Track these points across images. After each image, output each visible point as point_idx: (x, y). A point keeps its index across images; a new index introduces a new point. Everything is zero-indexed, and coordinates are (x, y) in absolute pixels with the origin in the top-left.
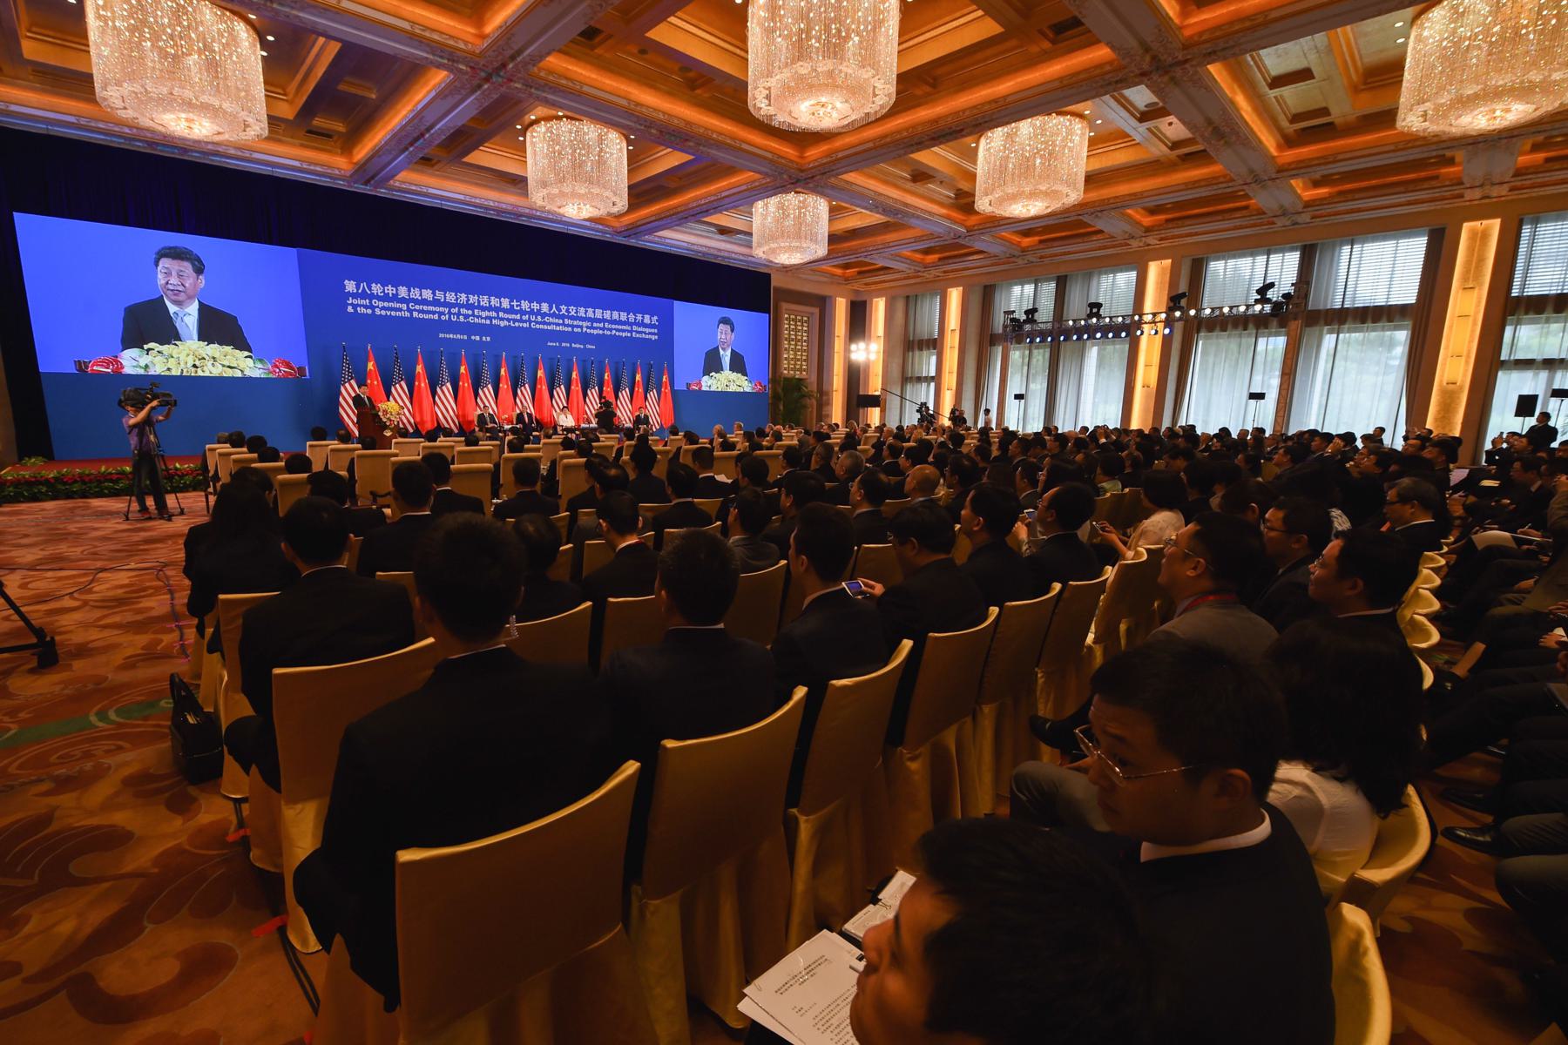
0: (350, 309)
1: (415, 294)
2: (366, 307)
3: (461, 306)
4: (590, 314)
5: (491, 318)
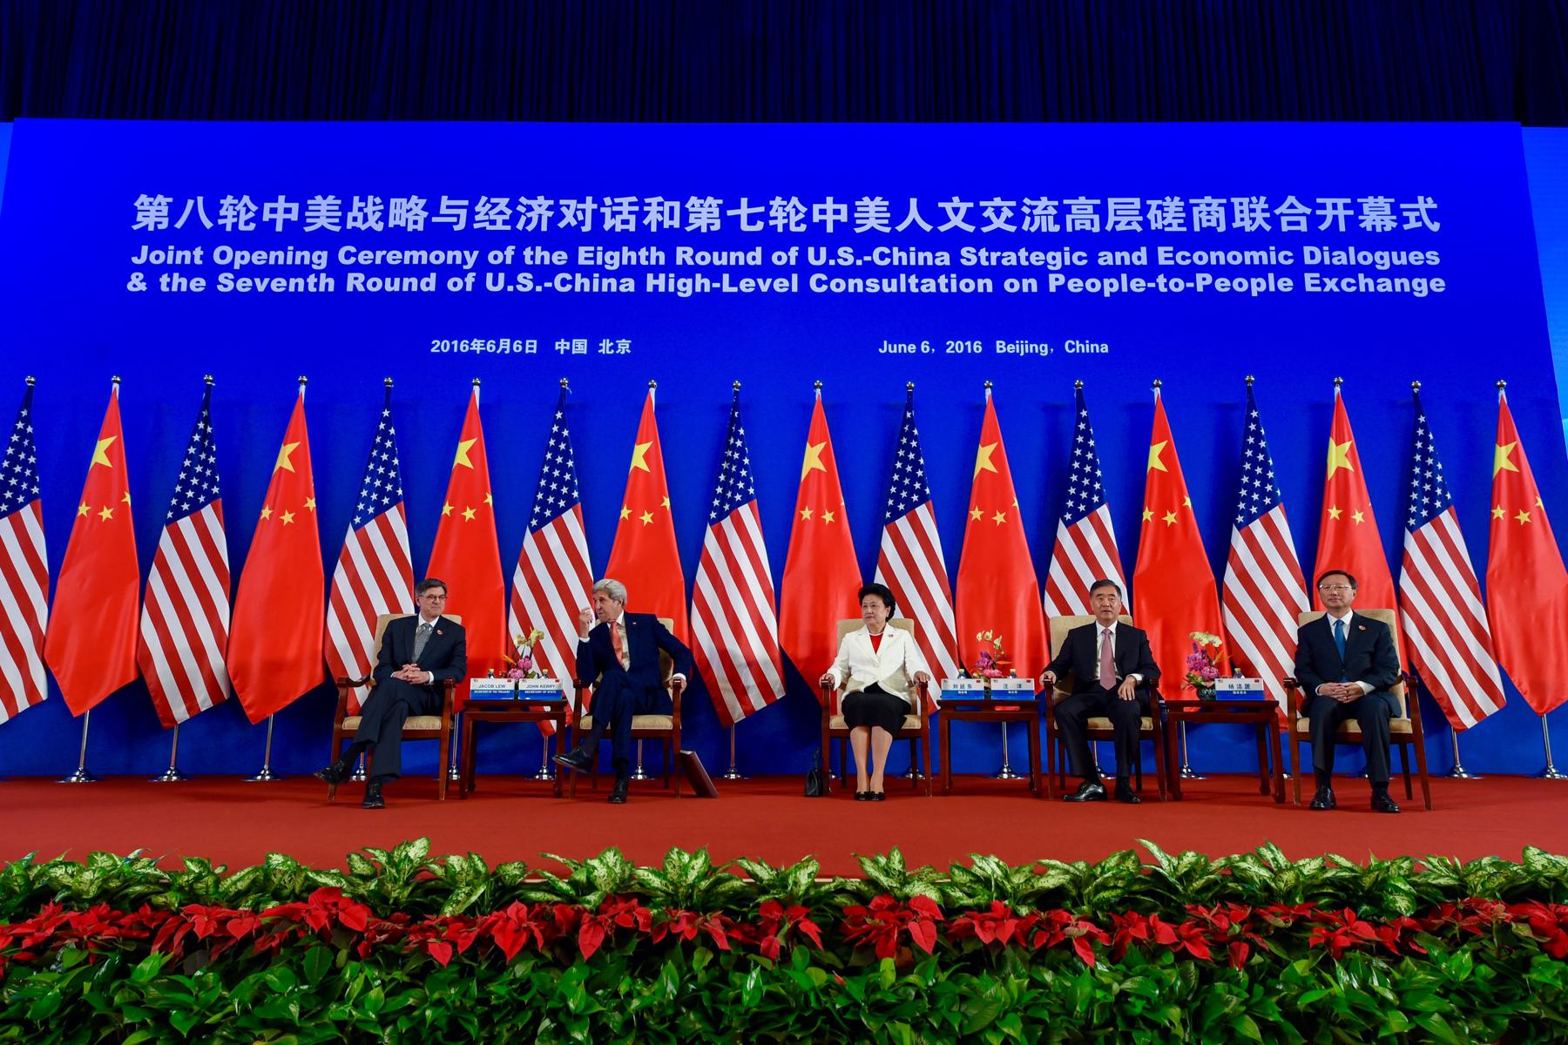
0: (137, 283)
1: (366, 214)
2: (188, 271)
3: (523, 240)
4: (1082, 214)
5: (638, 272)
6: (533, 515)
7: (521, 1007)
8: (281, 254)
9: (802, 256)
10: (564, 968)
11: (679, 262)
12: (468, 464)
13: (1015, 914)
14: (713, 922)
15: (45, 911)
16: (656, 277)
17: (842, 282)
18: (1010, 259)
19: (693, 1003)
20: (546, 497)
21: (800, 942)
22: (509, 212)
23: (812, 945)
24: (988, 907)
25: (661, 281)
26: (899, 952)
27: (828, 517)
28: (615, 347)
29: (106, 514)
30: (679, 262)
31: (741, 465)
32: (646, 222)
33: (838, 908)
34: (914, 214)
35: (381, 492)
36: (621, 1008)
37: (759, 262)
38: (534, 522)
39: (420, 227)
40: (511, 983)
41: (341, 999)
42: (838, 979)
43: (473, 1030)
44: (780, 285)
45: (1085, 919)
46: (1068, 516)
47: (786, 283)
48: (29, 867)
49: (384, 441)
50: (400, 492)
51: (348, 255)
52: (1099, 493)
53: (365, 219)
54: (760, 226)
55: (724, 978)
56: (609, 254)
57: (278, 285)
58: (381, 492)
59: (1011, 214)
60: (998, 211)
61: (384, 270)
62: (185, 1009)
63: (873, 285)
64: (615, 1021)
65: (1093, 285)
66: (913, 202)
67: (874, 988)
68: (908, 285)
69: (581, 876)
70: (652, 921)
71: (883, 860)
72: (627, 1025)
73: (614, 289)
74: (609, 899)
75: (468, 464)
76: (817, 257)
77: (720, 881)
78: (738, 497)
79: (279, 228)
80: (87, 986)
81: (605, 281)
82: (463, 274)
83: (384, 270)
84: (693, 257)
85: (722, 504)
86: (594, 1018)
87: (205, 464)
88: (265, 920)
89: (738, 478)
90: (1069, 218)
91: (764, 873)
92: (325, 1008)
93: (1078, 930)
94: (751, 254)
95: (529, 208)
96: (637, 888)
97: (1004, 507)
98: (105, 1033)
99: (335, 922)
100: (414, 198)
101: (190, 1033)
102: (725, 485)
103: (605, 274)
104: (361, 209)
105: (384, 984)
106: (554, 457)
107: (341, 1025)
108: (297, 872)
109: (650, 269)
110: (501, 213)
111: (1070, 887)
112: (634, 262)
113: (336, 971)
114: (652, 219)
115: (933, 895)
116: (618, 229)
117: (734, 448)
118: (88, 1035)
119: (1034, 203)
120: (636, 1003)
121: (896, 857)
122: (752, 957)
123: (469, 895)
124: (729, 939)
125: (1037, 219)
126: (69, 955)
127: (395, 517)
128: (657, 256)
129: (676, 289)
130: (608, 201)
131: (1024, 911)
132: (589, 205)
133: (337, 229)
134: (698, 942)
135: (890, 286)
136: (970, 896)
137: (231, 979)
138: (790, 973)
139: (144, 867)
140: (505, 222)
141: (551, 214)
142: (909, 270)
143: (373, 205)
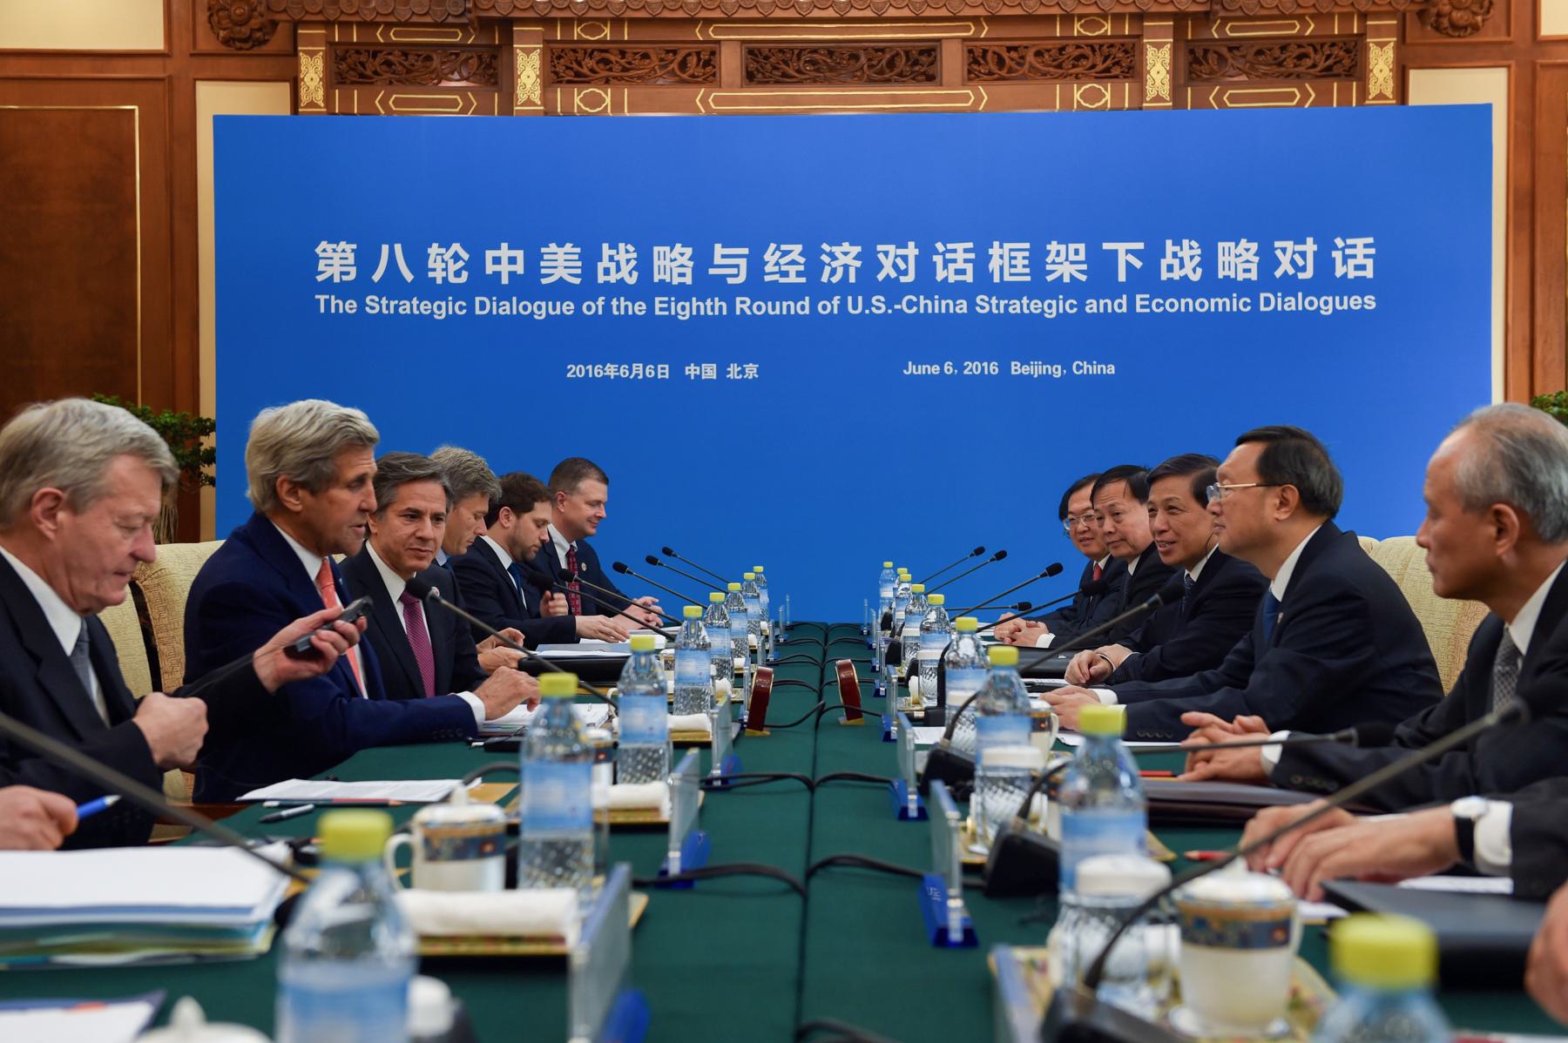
76: (855, 308)
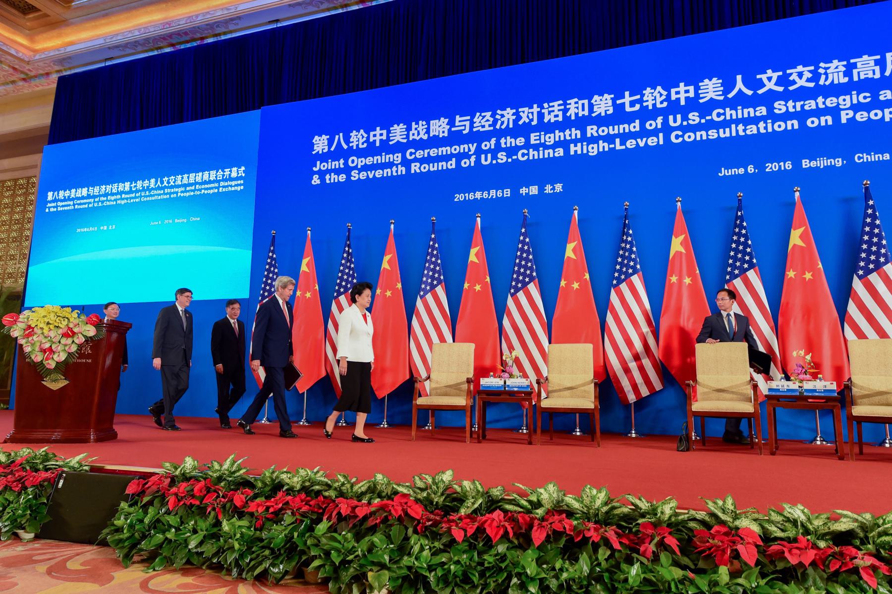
0: (316, 180)
1: (419, 131)
2: (338, 171)
6: (511, 287)
7: (501, 570)
8: (379, 157)
9: (665, 122)
10: (525, 550)
11: (589, 135)
12: (476, 261)
13: (815, 547)
14: (610, 533)
15: (280, 494)
16: (576, 146)
17: (692, 135)
18: (810, 105)
19: (599, 579)
20: (518, 276)
21: (666, 550)
22: (491, 119)
23: (673, 552)
24: (795, 540)
25: (579, 148)
26: (732, 563)
27: (687, 281)
28: (554, 189)
29: (308, 295)
30: (589, 135)
31: (631, 252)
32: (568, 114)
33: (690, 530)
34: (740, 85)
35: (433, 278)
36: (557, 577)
37: (638, 129)
38: (512, 291)
39: (446, 134)
40: (496, 555)
41: (409, 554)
42: (689, 574)
43: (475, 579)
44: (652, 141)
45: (870, 554)
46: (861, 272)
47: (655, 139)
48: (273, 472)
49: (433, 251)
50: (442, 277)
51: (411, 154)
52: (885, 255)
53: (419, 134)
54: (637, 107)
55: (617, 566)
56: (548, 135)
57: (379, 174)
58: (433, 278)
59: (810, 75)
60: (800, 75)
61: (429, 160)
62: (338, 551)
63: (713, 134)
64: (553, 584)
65: (875, 115)
66: (739, 78)
67: (716, 584)
68: (737, 131)
69: (534, 498)
70: (574, 528)
71: (720, 503)
72: (561, 586)
73: (551, 156)
74: (548, 512)
75: (476, 261)
76: (675, 121)
77: (614, 508)
78: (630, 271)
79: (378, 144)
80: (296, 534)
81: (546, 152)
82: (469, 157)
83: (429, 160)
84: (597, 131)
85: (620, 275)
86: (542, 580)
87: (349, 268)
88: (373, 509)
89: (630, 259)
90: (855, 72)
91: (644, 505)
92: (401, 559)
93: (863, 561)
94: (632, 125)
95: (502, 116)
96: (565, 508)
97: (813, 268)
98: (304, 558)
99: (406, 514)
100: (442, 119)
101: (340, 563)
102: (621, 264)
103: (546, 147)
104: (416, 129)
105: (430, 549)
106: (522, 254)
107: (409, 568)
108: (389, 484)
109: (572, 141)
110: (488, 120)
111: (858, 531)
112: (562, 139)
113: (407, 539)
114: (572, 113)
115: (755, 528)
116: (552, 121)
117: (626, 242)
118: (297, 558)
119: (827, 65)
120: (565, 575)
121: (730, 501)
122: (635, 555)
123: (473, 504)
124: (620, 543)
125: (830, 76)
126: (288, 518)
127: (440, 291)
128: (576, 133)
129: (588, 151)
130: (546, 105)
131: (822, 544)
132: (536, 109)
133: (405, 141)
134: (602, 543)
135: (724, 134)
136: (783, 530)
137: (358, 537)
138: (659, 568)
139: (320, 477)
140: (490, 126)
141: (514, 117)
142: (737, 122)
143: (422, 125)
